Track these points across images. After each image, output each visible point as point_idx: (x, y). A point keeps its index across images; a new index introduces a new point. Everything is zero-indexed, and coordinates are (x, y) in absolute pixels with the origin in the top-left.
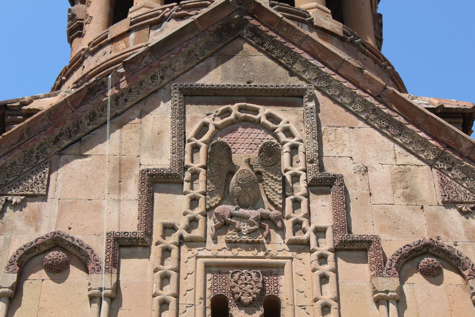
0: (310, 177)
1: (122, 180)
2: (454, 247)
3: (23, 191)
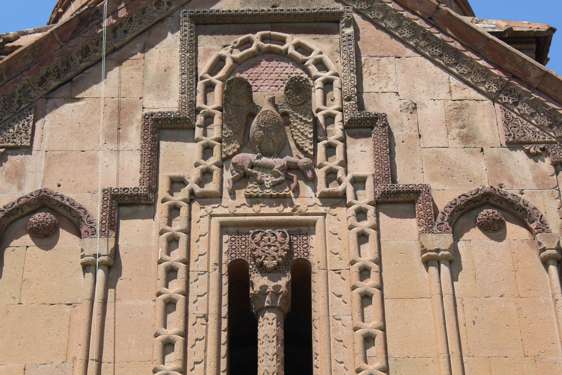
0: (347, 117)
1: (121, 127)
2: (520, 196)
3: (2, 143)
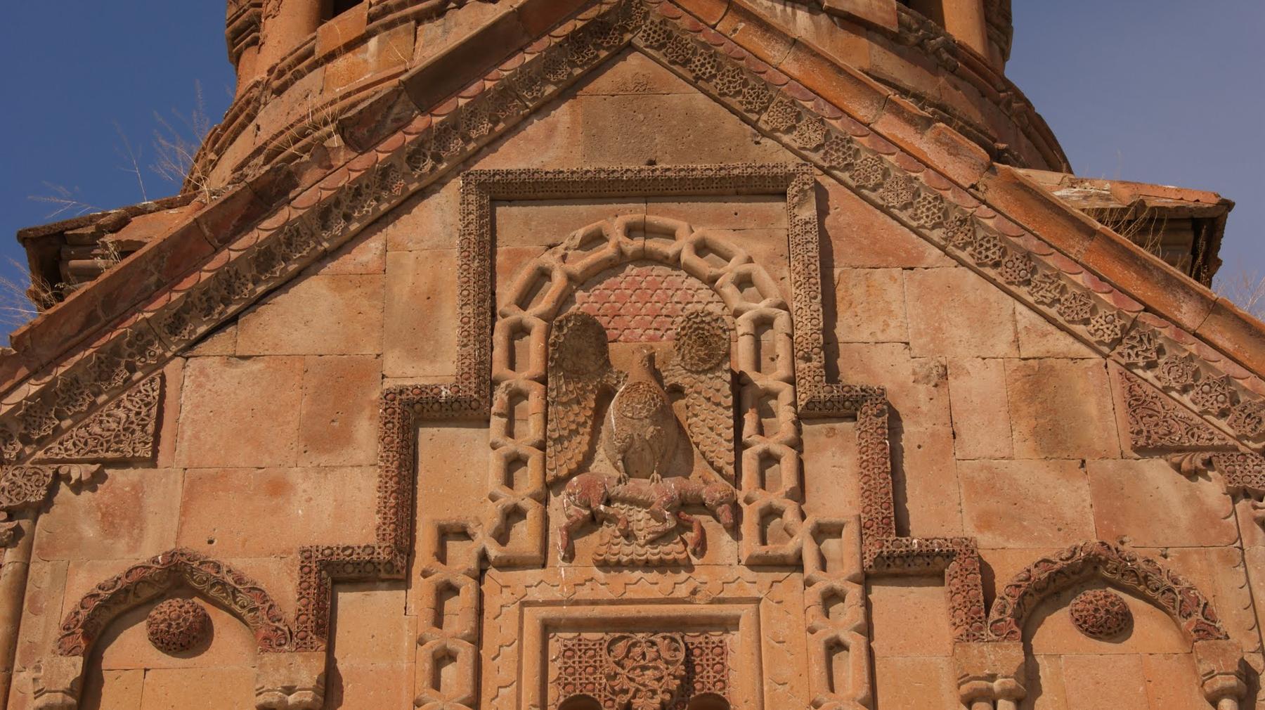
3: (96, 452)
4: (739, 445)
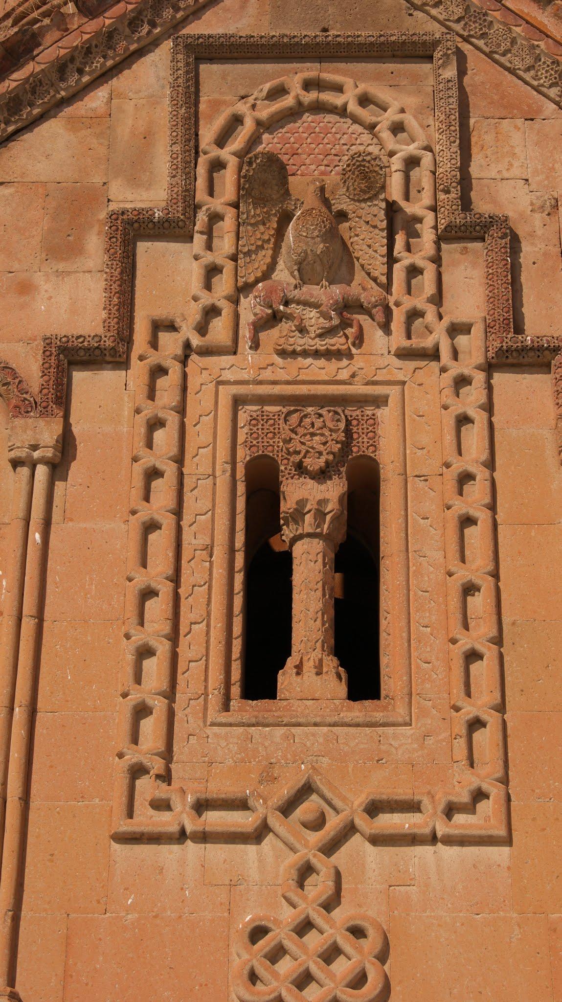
0: (443, 221)
4: (391, 260)
